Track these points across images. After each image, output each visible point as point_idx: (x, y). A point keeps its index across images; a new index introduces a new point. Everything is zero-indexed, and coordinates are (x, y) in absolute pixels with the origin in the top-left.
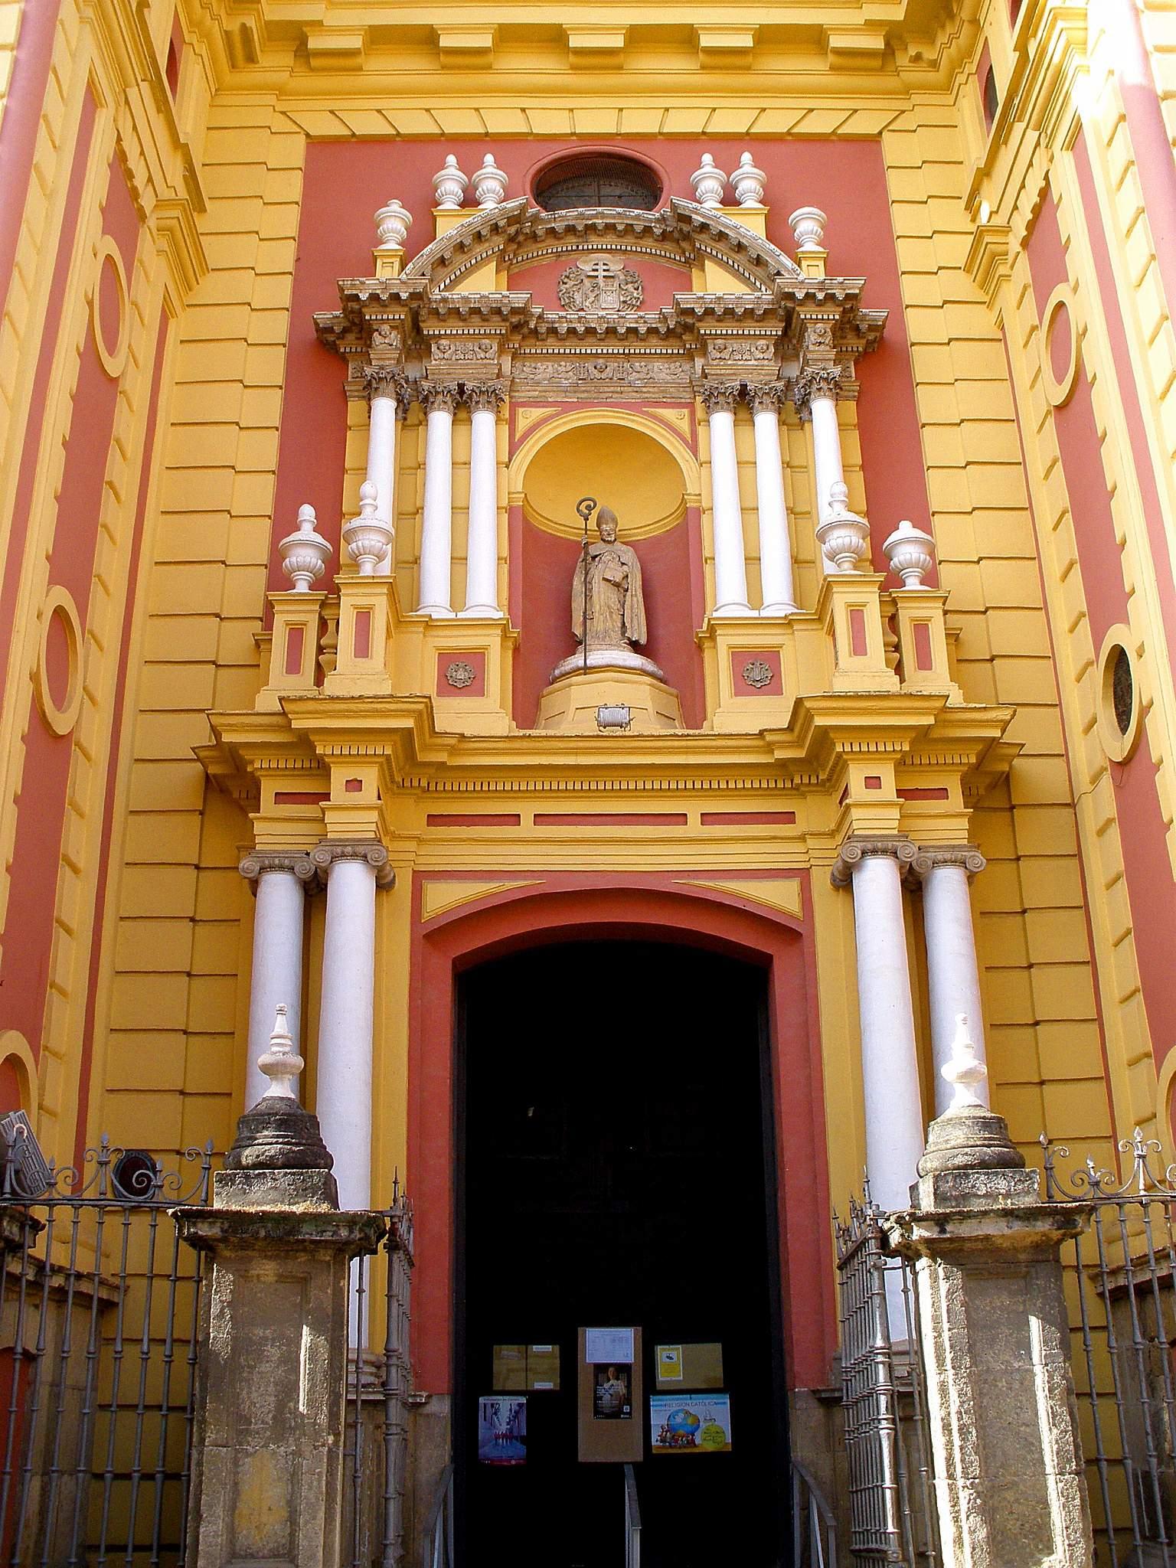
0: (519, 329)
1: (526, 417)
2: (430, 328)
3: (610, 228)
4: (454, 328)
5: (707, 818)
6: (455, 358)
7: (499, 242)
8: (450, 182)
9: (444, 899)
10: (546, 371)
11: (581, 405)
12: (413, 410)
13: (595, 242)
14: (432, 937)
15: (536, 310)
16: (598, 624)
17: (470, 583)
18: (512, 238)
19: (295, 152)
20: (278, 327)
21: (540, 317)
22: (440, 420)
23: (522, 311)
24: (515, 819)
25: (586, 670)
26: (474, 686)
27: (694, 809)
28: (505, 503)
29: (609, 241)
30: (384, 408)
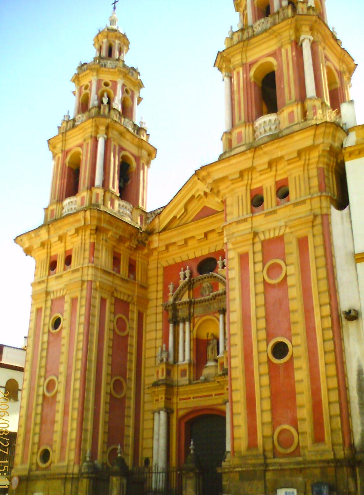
0: (191, 304)
1: (196, 320)
2: (178, 307)
3: (205, 278)
4: (181, 307)
5: (216, 395)
6: (183, 313)
7: (187, 287)
8: (182, 273)
9: (181, 413)
10: (198, 310)
11: (204, 315)
12: (176, 324)
13: (205, 280)
14: (179, 420)
15: (193, 300)
16: (210, 357)
17: (185, 355)
18: (190, 285)
19: (161, 272)
20: (160, 309)
21: (194, 301)
22: (181, 325)
23: (191, 301)
24: (189, 398)
25: (206, 367)
26: (185, 375)
27: (213, 393)
28: (192, 338)
29: (207, 279)
30: (171, 326)
